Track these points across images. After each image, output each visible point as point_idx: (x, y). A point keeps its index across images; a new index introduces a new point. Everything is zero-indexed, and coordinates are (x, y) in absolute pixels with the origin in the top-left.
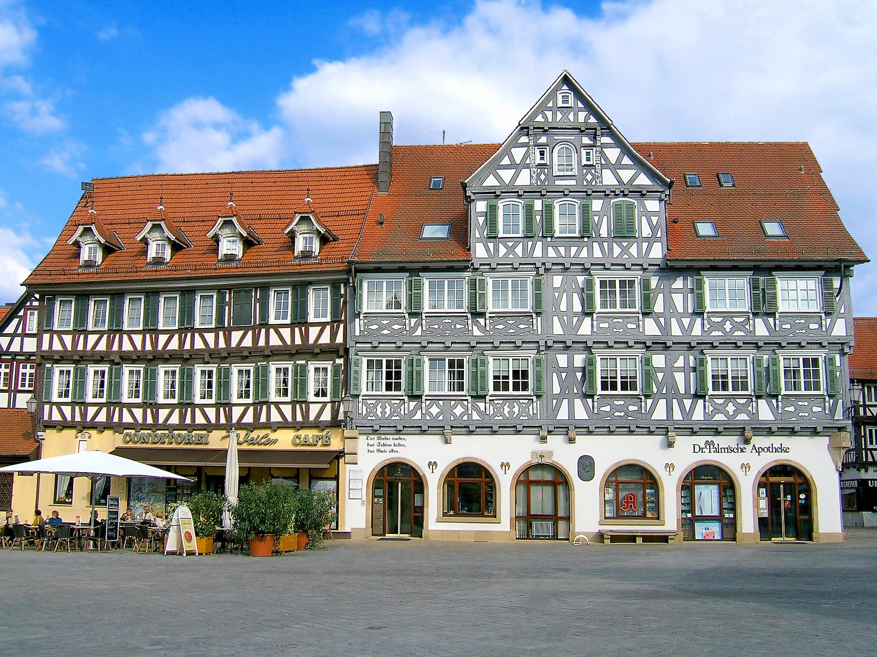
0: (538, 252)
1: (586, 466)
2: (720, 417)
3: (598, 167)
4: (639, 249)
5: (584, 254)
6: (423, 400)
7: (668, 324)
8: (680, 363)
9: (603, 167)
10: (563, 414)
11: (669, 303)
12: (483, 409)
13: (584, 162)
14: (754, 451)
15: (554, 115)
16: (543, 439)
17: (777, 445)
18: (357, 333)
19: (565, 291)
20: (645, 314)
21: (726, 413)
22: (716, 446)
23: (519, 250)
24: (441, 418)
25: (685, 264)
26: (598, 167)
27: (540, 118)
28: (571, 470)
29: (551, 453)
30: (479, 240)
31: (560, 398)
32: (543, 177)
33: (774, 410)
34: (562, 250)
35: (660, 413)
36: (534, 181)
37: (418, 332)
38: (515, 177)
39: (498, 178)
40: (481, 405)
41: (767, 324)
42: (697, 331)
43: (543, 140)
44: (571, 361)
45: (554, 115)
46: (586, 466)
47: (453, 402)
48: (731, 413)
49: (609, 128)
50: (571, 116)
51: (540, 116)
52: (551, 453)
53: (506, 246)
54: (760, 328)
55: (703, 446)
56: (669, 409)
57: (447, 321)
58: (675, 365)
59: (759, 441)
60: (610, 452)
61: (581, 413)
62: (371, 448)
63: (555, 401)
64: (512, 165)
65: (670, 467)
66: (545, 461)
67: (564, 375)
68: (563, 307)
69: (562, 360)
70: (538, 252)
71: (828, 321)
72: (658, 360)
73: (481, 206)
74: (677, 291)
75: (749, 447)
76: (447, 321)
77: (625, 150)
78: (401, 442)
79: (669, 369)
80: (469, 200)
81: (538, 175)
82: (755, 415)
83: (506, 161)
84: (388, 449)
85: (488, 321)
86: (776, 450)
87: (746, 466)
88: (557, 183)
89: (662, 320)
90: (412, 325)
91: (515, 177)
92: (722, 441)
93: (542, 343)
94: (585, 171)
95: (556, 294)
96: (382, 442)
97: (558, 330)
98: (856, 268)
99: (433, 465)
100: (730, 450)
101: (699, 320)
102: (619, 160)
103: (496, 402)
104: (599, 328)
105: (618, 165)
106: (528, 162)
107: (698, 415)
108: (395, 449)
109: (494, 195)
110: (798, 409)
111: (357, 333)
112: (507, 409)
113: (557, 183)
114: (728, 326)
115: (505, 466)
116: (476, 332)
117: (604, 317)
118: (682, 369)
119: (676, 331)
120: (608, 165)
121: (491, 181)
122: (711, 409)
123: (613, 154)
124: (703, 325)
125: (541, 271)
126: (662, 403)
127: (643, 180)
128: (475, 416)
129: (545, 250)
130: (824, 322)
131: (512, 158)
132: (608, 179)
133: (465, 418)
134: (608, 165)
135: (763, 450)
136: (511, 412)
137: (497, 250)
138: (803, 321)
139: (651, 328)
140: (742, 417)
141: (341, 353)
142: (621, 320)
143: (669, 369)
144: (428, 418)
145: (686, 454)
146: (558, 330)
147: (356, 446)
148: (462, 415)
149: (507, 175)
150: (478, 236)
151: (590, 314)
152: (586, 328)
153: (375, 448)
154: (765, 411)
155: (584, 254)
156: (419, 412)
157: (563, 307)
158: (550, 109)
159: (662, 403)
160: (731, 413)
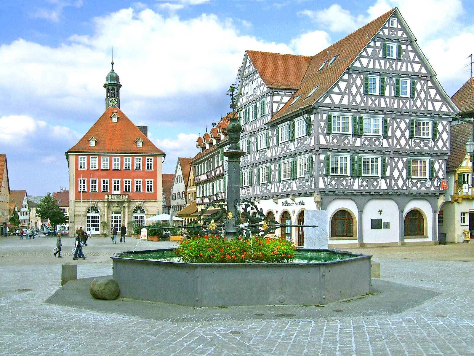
2: (285, 190)
17: (301, 202)
27: (245, 74)
34: (252, 126)
59: (298, 200)
71: (310, 138)
75: (295, 203)
87: (294, 211)
88: (250, 99)
92: (289, 200)
105: (261, 85)
113: (250, 99)
140: (289, 189)
159: (273, 184)
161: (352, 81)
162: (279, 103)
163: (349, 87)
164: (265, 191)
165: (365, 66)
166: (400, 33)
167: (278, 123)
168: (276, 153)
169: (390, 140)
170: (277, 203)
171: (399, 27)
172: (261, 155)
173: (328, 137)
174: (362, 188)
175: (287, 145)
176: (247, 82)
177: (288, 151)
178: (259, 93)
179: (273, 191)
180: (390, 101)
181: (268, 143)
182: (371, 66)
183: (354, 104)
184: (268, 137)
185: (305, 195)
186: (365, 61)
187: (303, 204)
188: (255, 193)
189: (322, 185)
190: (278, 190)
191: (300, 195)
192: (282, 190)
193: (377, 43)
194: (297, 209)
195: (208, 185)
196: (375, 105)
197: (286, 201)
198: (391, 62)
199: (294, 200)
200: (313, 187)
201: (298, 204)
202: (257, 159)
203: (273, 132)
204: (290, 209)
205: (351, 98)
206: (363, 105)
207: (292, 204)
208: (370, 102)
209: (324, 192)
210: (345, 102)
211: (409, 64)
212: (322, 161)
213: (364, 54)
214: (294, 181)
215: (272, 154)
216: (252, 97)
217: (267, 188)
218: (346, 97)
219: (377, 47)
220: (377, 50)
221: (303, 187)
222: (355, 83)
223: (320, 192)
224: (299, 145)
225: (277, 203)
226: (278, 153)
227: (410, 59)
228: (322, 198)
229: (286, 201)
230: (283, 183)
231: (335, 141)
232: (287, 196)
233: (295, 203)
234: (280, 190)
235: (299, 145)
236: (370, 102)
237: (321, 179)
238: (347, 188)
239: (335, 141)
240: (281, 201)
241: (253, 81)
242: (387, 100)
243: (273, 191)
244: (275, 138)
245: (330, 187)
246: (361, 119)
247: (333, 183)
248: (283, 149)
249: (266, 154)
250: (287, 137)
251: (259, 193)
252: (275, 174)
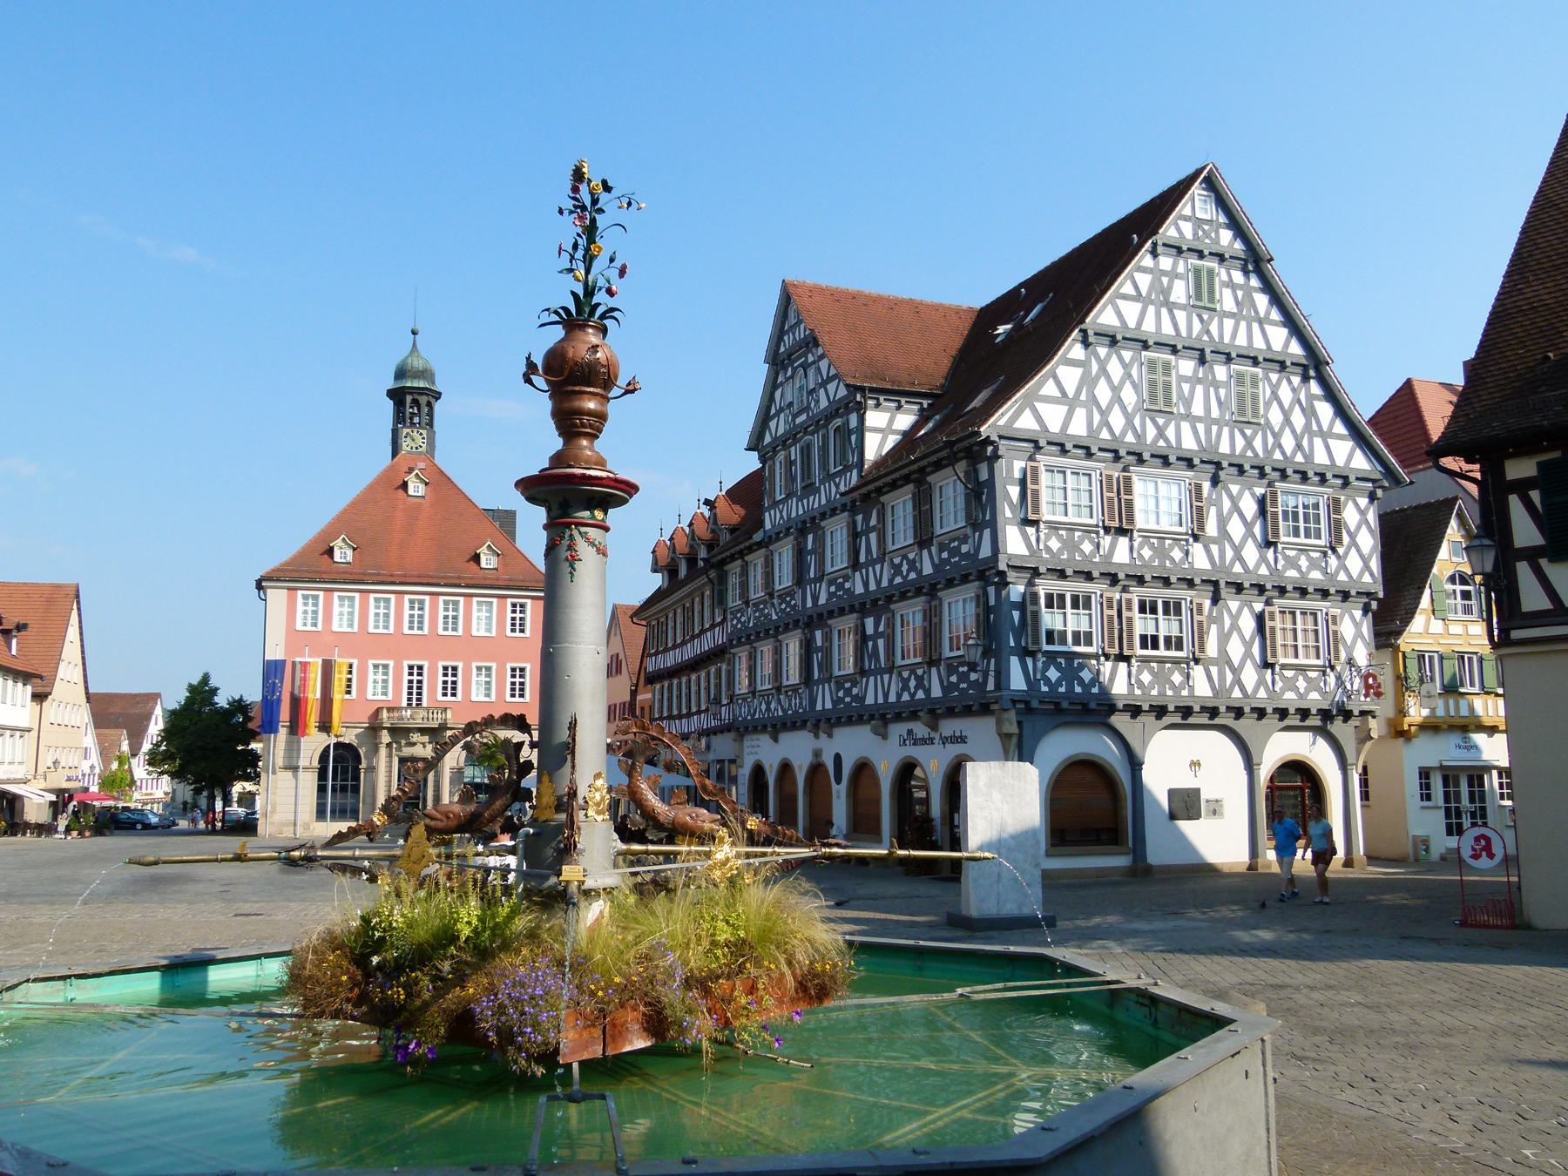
2: (906, 697)
13: (812, 386)
16: (817, 736)
27: (782, 349)
59: (949, 727)
72: (869, 623)
75: (937, 736)
79: (877, 635)
88: (798, 421)
113: (798, 421)
114: (905, 568)
140: (920, 695)
158: (787, 332)
161: (1095, 367)
162: (884, 432)
163: (1088, 382)
164: (848, 699)
165: (1132, 324)
166: (1226, 236)
167: (879, 491)
168: (878, 582)
169: (1214, 548)
170: (885, 737)
171: (1222, 219)
172: (833, 589)
173: (1031, 530)
174: (1138, 692)
175: (911, 556)
176: (789, 373)
177: (913, 575)
178: (824, 403)
179: (870, 700)
180: (1208, 432)
181: (854, 551)
182: (1149, 326)
183: (1105, 435)
184: (855, 535)
185: (967, 711)
186: (1131, 311)
188: (819, 707)
189: (1017, 682)
190: (886, 696)
191: (951, 713)
192: (899, 696)
193: (1161, 258)
195: (675, 682)
196: (1167, 440)
197: (910, 732)
198: (1205, 317)
199: (934, 728)
200: (991, 686)
201: (944, 740)
202: (822, 601)
203: (866, 520)
205: (1097, 417)
206: (1130, 438)
207: (931, 741)
208: (1151, 432)
209: (1027, 703)
210: (1078, 428)
211: (1255, 326)
212: (1016, 606)
213: (1128, 289)
214: (934, 670)
215: (866, 584)
216: (803, 417)
217: (855, 691)
218: (1080, 414)
219: (1164, 273)
220: (1165, 280)
222: (1103, 371)
223: (1014, 702)
224: (945, 555)
225: (885, 737)
226: (885, 583)
227: (1257, 312)
228: (1020, 723)
229: (910, 732)
230: (900, 674)
231: (1054, 544)
232: (914, 716)
233: (937, 736)
234: (892, 698)
235: (945, 555)
236: (1151, 432)
237: (1014, 661)
238: (1095, 690)
239: (1054, 544)
240: (898, 730)
241: (805, 366)
242: (1201, 427)
243: (870, 700)
244: (873, 536)
245: (1045, 689)
246: (1128, 481)
247: (1053, 674)
248: (897, 569)
249: (847, 585)
250: (910, 533)
251: (829, 705)
252: (875, 646)
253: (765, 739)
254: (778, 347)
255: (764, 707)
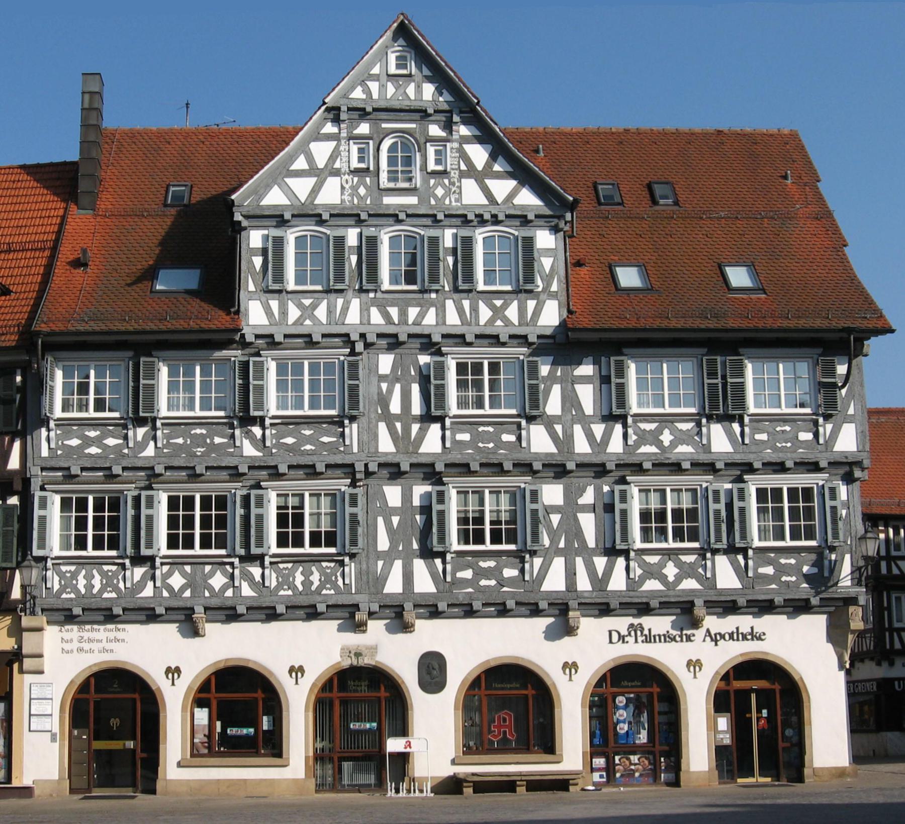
0: (353, 317)
1: (433, 671)
2: (653, 585)
3: (455, 175)
4: (522, 310)
5: (430, 318)
6: (158, 564)
7: (569, 437)
8: (588, 497)
9: (463, 175)
10: (394, 585)
11: (570, 401)
12: (258, 578)
13: (432, 166)
14: (708, 639)
15: (383, 87)
17: (745, 629)
18: (45, 453)
19: (398, 380)
20: (531, 419)
21: (663, 579)
22: (646, 632)
23: (321, 313)
24: (187, 594)
25: (596, 336)
26: (455, 175)
28: (408, 674)
29: (374, 649)
30: (252, 296)
31: (389, 557)
32: (362, 191)
33: (742, 572)
34: (394, 312)
35: (555, 582)
36: (346, 198)
37: (150, 451)
38: (315, 191)
39: (289, 192)
40: (256, 571)
41: (730, 434)
42: (616, 446)
43: (364, 128)
44: (407, 496)
45: (383, 87)
46: (433, 671)
47: (208, 568)
48: (671, 578)
49: (473, 111)
50: (411, 90)
51: (359, 89)
52: (374, 649)
53: (300, 306)
54: (720, 440)
55: (624, 632)
56: (571, 575)
57: (198, 431)
58: (581, 501)
60: (472, 645)
61: (424, 583)
62: (67, 647)
63: (380, 563)
64: (312, 171)
65: (570, 667)
66: (366, 661)
67: (395, 520)
68: (395, 407)
69: (393, 494)
70: (353, 317)
71: (829, 427)
72: (552, 493)
73: (255, 238)
74: (585, 380)
75: (699, 633)
76: (198, 431)
77: (498, 148)
78: (120, 635)
79: (570, 509)
80: (238, 229)
81: (355, 188)
82: (710, 582)
83: (301, 163)
84: (95, 646)
85: (268, 432)
86: (745, 637)
87: (697, 664)
88: (388, 200)
89: (559, 428)
90: (139, 438)
91: (315, 191)
92: (660, 624)
93: (360, 467)
94: (432, 182)
95: (384, 386)
96: (86, 635)
97: (386, 445)
98: (873, 344)
99: (173, 672)
100: (668, 638)
101: (618, 428)
102: (488, 166)
103: (281, 566)
104: (455, 442)
106: (337, 165)
107: (618, 582)
108: (109, 646)
109: (279, 219)
110: (781, 570)
111: (45, 453)
112: (299, 579)
113: (388, 200)
114: (666, 437)
115: (296, 671)
116: (249, 450)
117: (463, 423)
118: (593, 508)
119: (582, 446)
120: (471, 172)
121: (275, 198)
122: (639, 572)
123: (479, 154)
124: (625, 436)
125: (359, 347)
126: (559, 564)
127: (527, 199)
128: (247, 591)
129: (365, 311)
130: (821, 429)
131: (310, 159)
132: (471, 195)
133: (229, 593)
134: (471, 172)
135: (723, 637)
136: (307, 583)
137: (284, 312)
138: (788, 428)
139: (540, 441)
140: (690, 584)
141: (18, 486)
142: (491, 429)
143: (570, 509)
144: (165, 594)
145: (596, 646)
146: (386, 445)
147: (41, 644)
148: (224, 588)
149: (302, 187)
150: (252, 287)
151: (441, 419)
152: (432, 443)
153: (75, 645)
154: (726, 575)
155: (430, 318)
156: (150, 584)
157: (395, 407)
158: (376, 78)
159: (559, 564)
160: (671, 578)
164: (483, 582)
187: (755, 636)
194: (719, 657)
204: (671, 657)
221: (784, 579)
253: (169, 632)
254: (353, 88)
255: (177, 581)
